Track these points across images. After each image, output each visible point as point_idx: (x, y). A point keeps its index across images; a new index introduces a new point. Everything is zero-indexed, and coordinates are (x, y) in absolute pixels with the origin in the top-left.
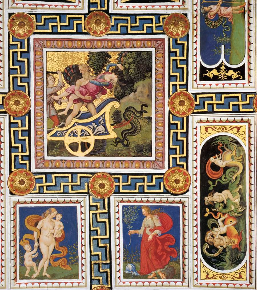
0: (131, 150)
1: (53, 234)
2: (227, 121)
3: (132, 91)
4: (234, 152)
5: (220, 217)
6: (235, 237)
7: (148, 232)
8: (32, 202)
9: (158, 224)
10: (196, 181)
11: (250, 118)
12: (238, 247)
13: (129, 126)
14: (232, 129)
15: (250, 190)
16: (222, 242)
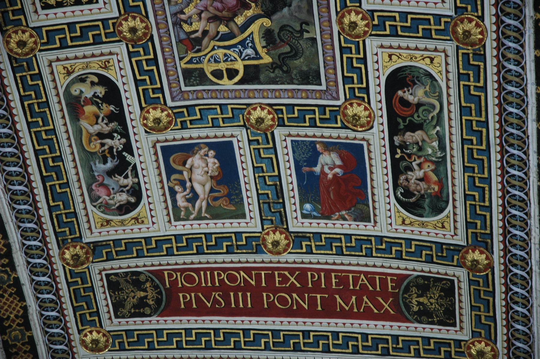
0: (293, 76)
1: (208, 172)
2: (417, 49)
3: (285, 5)
4: (428, 87)
5: (415, 160)
6: (435, 183)
7: (326, 170)
8: (174, 140)
9: (338, 162)
10: (382, 116)
11: (447, 48)
12: (439, 195)
13: (287, 49)
14: (423, 59)
15: (451, 134)
16: (418, 188)
